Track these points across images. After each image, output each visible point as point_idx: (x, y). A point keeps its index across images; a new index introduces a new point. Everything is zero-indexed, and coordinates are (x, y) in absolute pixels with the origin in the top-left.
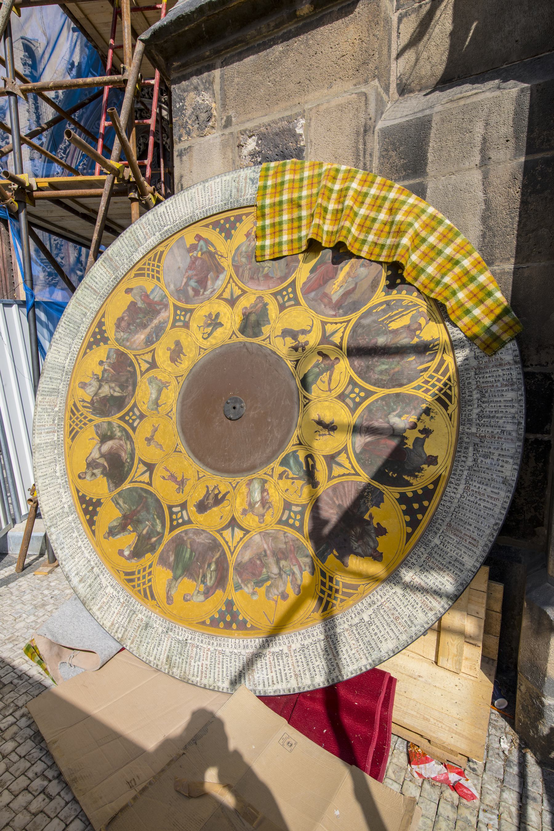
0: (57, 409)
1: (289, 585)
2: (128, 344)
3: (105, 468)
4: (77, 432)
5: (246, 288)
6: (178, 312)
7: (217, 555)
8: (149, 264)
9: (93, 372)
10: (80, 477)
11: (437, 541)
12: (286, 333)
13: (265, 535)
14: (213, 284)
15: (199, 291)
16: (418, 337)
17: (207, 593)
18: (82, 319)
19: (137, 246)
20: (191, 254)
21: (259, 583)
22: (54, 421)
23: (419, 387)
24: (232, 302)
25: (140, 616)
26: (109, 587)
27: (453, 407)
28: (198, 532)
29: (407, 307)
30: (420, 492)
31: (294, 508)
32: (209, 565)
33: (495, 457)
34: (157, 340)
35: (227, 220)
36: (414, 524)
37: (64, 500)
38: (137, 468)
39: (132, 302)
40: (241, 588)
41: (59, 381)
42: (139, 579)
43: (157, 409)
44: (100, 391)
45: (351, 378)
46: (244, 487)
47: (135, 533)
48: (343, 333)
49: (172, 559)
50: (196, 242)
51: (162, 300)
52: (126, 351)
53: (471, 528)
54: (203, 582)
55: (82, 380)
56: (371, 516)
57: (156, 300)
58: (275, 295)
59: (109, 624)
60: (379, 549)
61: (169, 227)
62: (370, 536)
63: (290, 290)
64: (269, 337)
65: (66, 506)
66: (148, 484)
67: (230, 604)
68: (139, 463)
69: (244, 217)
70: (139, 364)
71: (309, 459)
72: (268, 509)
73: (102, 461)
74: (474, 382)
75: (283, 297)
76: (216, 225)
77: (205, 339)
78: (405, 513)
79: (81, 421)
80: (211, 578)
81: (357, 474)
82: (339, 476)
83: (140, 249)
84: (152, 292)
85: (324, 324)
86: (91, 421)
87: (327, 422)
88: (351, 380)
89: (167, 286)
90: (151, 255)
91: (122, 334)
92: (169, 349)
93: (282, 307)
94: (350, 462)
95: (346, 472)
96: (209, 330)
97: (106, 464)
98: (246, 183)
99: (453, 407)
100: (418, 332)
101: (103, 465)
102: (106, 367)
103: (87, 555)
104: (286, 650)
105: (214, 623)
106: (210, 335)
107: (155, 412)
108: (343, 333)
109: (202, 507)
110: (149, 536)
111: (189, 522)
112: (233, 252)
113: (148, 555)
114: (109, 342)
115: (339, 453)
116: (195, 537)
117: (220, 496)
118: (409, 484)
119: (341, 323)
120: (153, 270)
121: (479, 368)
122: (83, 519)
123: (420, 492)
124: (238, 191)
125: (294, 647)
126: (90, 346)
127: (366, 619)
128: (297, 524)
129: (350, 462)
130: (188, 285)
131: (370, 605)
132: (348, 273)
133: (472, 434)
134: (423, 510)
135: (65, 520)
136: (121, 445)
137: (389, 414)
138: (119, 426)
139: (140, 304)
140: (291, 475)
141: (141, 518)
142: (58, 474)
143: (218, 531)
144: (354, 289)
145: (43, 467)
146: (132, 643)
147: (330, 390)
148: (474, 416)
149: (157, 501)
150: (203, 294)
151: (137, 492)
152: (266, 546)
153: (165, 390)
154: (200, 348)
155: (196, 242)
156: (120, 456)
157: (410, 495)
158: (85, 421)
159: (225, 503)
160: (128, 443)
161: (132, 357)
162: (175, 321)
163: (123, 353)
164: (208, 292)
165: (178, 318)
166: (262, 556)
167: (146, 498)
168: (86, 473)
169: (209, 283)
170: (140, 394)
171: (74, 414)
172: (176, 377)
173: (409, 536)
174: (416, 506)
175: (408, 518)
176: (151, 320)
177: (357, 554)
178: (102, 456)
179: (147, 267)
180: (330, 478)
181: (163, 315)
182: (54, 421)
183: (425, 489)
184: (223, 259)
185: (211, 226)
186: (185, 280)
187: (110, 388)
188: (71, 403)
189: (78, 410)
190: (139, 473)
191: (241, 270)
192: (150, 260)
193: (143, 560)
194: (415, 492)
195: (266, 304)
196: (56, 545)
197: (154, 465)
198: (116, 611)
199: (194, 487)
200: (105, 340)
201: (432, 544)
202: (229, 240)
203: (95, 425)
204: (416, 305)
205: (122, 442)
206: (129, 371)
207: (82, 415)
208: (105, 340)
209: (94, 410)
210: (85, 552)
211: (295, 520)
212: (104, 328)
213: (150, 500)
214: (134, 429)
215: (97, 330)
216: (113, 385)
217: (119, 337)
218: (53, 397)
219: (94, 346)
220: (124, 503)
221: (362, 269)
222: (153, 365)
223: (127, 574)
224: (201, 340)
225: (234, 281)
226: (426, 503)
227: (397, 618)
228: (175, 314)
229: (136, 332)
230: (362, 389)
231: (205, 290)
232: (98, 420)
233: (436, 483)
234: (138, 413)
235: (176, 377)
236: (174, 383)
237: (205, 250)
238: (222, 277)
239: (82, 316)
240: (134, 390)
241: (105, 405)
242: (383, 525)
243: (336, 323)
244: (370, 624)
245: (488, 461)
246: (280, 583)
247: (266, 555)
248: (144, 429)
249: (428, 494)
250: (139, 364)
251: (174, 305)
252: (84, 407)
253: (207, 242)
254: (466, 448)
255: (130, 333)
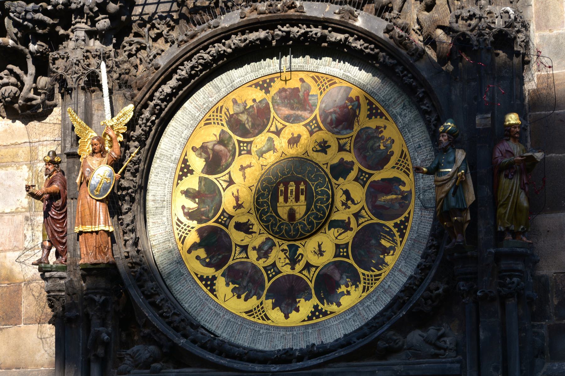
0: (211, 99)
1: (245, 294)
2: (276, 107)
3: (209, 157)
4: (210, 123)
5: (352, 151)
6: (314, 122)
7: (227, 254)
8: (324, 80)
9: (245, 101)
10: (193, 148)
11: (310, 331)
12: (346, 193)
13: (254, 266)
14: (342, 129)
15: (333, 125)
16: (384, 256)
17: (208, 265)
18: (266, 66)
19: (328, 64)
20: (347, 102)
21: (233, 283)
22: (204, 104)
23: (364, 274)
24: (341, 148)
25: (171, 244)
26: (166, 218)
27: (365, 294)
28: (227, 236)
29: (394, 241)
30: (324, 310)
31: (275, 269)
32: (219, 255)
33: (356, 324)
34: (293, 122)
35: (377, 108)
36: (310, 318)
37: (175, 152)
38: (225, 175)
39: (298, 88)
40: (224, 277)
41: (225, 86)
42: (182, 228)
43: (259, 158)
44: (240, 115)
45: (348, 243)
46: (265, 238)
47: (197, 206)
48: (365, 221)
49: (205, 235)
50: (355, 100)
51: (312, 106)
52: (272, 109)
53: (325, 338)
54: (210, 258)
55: (237, 99)
56: (299, 301)
57: (310, 102)
58: (360, 170)
59: (153, 234)
60: (290, 315)
61: (350, 75)
62: (292, 307)
63: (367, 176)
64: (339, 185)
65: (174, 156)
66: (223, 188)
67: (214, 278)
68: (227, 174)
69: (384, 117)
70: (272, 124)
71: (301, 256)
72: (265, 258)
73: (210, 152)
74: (379, 293)
75: (362, 175)
76: (370, 103)
77: (313, 150)
78: (311, 312)
79: (217, 119)
80: (215, 260)
81: (311, 281)
82: (304, 275)
83: (327, 67)
84: (312, 95)
85: (363, 208)
86: (222, 125)
87: (322, 250)
88: (348, 244)
89: (322, 102)
90: (330, 78)
91: (278, 98)
92: (292, 134)
93: (356, 179)
94: (313, 275)
95: (309, 277)
96: (319, 148)
97: (211, 156)
98: (401, 103)
99: (365, 294)
100: (386, 254)
101: (209, 155)
102: (255, 106)
103: (166, 192)
104: (221, 315)
105: (201, 279)
106: (317, 151)
107: (258, 158)
108: (365, 221)
109: (239, 227)
110: (203, 214)
111: (227, 227)
112: (364, 126)
113: (195, 222)
114: (268, 94)
115: (314, 266)
116: (223, 236)
117: (251, 230)
118: (323, 304)
119: (369, 216)
120: (323, 86)
121: (386, 291)
122: (179, 173)
123: (324, 310)
124: (394, 102)
125: (226, 317)
126: (257, 85)
127: (261, 332)
128: (271, 276)
129: (313, 275)
130: (331, 115)
131: (267, 329)
132: (392, 199)
133: (359, 310)
134: (318, 317)
135: (168, 163)
136: (227, 155)
137: (345, 272)
138: (234, 144)
139: (301, 94)
140: (287, 254)
141: (206, 201)
142: (183, 135)
143: (236, 245)
144: (387, 209)
145: (178, 123)
146: (158, 252)
147: (336, 238)
148: (366, 305)
149: (221, 202)
150: (333, 128)
151: (214, 187)
152: (250, 271)
153: (272, 152)
154: (307, 152)
155: (355, 100)
156: (221, 160)
157: (320, 308)
158: (220, 122)
159: (250, 236)
160: (231, 158)
161: (272, 117)
162: (308, 124)
163: (269, 109)
164: (336, 130)
165: (311, 124)
166: (245, 273)
167: (217, 194)
168: (197, 149)
169: (341, 126)
170: (259, 140)
171: (217, 112)
172: (283, 152)
173: (304, 321)
174: (317, 313)
175: (310, 315)
176: (298, 109)
177: (281, 309)
178: (213, 150)
179: (322, 80)
180: (300, 272)
181: (305, 114)
182: (204, 104)
183: (326, 311)
184: (357, 124)
185: (368, 101)
186: (332, 110)
187: (247, 119)
188: (220, 105)
189: (221, 112)
190: (224, 178)
191: (358, 140)
192: (327, 78)
193: (191, 221)
194: (322, 309)
195: (353, 170)
196: (154, 171)
197: (234, 183)
198: (161, 232)
199: (243, 214)
200: (267, 92)
201: (308, 331)
202: (368, 119)
203: (222, 130)
204: (397, 244)
205: (228, 154)
206: (264, 122)
207: (221, 116)
208: (267, 92)
209: (229, 121)
210: (166, 189)
211: (271, 273)
212: (272, 84)
213: (217, 197)
214: (240, 154)
215: (268, 81)
216: (250, 119)
217: (275, 98)
218: (214, 90)
219: (259, 88)
220: (204, 185)
221: (398, 205)
222: (278, 133)
223: (178, 220)
224: (311, 149)
225: (351, 140)
226: (321, 316)
227: (271, 341)
228: (312, 121)
229: (286, 106)
230: (347, 252)
231: (336, 127)
232: (226, 129)
233: (331, 313)
234: (249, 148)
235: (283, 152)
236: (279, 154)
237: (354, 108)
238: (348, 131)
239: (267, 65)
240: (257, 135)
241: (237, 125)
242: (300, 309)
243: (367, 214)
244: (261, 335)
245: (353, 323)
246: (242, 291)
247: (246, 274)
248: (244, 160)
249: (325, 314)
250: (272, 124)
251: (316, 116)
252: (225, 113)
253: (359, 106)
254: (352, 312)
255: (282, 103)
